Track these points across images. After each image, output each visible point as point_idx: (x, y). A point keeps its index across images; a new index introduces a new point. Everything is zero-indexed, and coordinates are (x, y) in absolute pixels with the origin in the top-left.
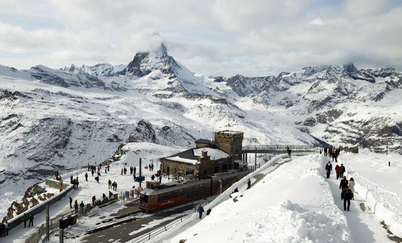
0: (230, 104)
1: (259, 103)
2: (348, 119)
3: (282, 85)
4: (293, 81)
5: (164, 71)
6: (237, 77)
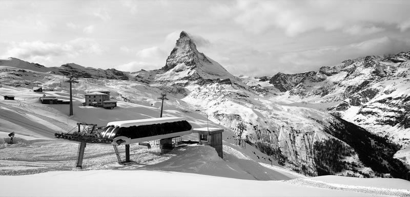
0: (235, 84)
1: (295, 94)
2: (385, 96)
3: (319, 76)
4: (330, 72)
5: (188, 64)
6: (278, 75)
